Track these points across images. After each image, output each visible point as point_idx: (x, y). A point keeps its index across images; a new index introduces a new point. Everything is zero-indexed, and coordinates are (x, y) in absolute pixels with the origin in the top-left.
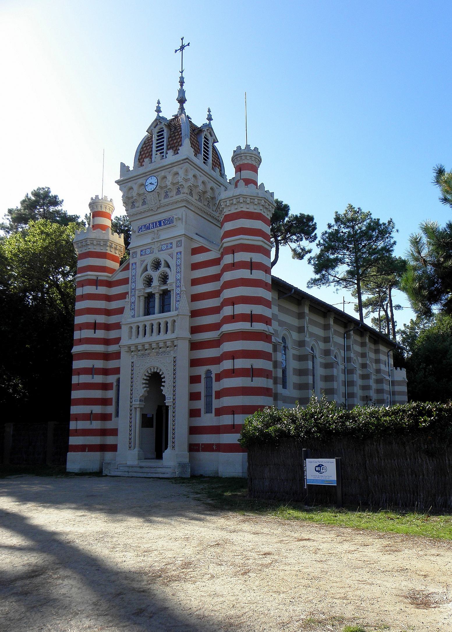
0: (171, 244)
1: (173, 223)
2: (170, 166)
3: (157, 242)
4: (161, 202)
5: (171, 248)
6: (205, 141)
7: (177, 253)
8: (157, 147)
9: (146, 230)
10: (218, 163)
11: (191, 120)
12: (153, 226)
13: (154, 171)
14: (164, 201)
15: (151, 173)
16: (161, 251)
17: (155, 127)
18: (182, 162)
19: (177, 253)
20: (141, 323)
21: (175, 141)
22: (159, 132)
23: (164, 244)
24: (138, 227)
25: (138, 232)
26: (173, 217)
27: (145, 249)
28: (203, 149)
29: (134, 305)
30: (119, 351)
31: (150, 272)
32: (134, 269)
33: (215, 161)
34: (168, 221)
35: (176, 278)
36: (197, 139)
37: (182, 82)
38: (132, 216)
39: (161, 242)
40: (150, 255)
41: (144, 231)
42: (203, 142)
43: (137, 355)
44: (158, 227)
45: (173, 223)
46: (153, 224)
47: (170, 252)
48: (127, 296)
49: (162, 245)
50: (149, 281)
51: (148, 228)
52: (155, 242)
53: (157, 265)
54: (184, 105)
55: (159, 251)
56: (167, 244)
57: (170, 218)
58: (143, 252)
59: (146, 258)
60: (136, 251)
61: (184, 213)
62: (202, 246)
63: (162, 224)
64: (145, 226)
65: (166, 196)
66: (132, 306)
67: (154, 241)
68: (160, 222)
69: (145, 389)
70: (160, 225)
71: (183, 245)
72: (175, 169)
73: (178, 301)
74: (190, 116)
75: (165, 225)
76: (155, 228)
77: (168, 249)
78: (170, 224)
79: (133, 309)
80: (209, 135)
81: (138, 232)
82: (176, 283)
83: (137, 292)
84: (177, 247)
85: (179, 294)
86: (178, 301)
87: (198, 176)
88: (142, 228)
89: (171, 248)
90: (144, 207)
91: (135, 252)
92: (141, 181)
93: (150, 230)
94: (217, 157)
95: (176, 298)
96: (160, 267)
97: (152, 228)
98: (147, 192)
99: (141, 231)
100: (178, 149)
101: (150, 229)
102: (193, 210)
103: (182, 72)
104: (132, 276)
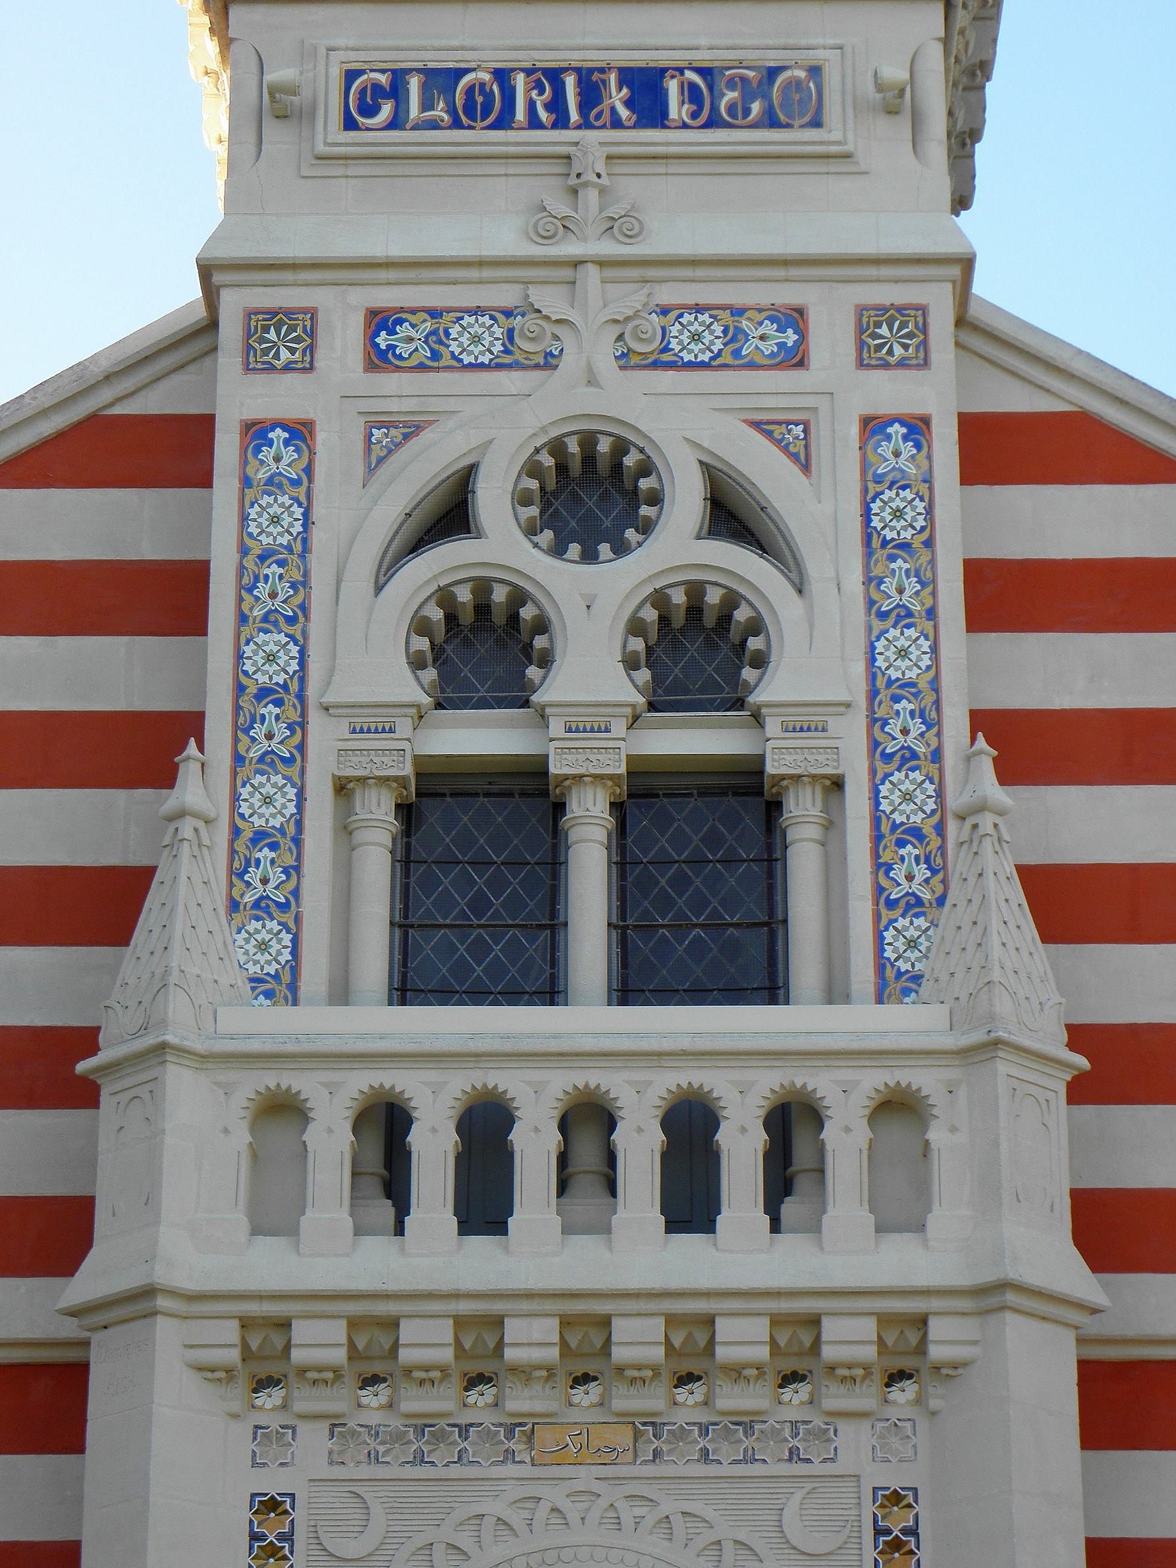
1: (816, 123)
3: (603, 263)
5: (796, 359)
9: (457, 124)
12: (557, 105)
16: (656, 365)
20: (433, 1076)
24: (351, 76)
25: (350, 124)
26: (815, 71)
27: (434, 313)
29: (294, 870)
30: (71, 1355)
32: (272, 482)
34: (749, 92)
35: (872, 678)
39: (652, 273)
41: (434, 125)
43: (335, 1425)
44: (617, 124)
47: (783, 402)
48: (192, 748)
49: (664, 311)
52: (576, 264)
55: (625, 360)
56: (737, 312)
57: (772, 73)
58: (404, 330)
59: (451, 405)
60: (313, 313)
63: (676, 108)
66: (254, 875)
67: (571, 248)
73: (914, 905)
75: (713, 122)
76: (586, 124)
77: (752, 366)
78: (771, 121)
79: (262, 907)
81: (350, 124)
82: (875, 721)
84: (861, 364)
85: (916, 833)
86: (914, 905)
88: (396, 90)
89: (796, 359)
91: (289, 313)
93: (510, 133)
95: (881, 867)
96: (646, 528)
97: (534, 123)
99: (394, 124)
101: (504, 121)
104: (244, 551)
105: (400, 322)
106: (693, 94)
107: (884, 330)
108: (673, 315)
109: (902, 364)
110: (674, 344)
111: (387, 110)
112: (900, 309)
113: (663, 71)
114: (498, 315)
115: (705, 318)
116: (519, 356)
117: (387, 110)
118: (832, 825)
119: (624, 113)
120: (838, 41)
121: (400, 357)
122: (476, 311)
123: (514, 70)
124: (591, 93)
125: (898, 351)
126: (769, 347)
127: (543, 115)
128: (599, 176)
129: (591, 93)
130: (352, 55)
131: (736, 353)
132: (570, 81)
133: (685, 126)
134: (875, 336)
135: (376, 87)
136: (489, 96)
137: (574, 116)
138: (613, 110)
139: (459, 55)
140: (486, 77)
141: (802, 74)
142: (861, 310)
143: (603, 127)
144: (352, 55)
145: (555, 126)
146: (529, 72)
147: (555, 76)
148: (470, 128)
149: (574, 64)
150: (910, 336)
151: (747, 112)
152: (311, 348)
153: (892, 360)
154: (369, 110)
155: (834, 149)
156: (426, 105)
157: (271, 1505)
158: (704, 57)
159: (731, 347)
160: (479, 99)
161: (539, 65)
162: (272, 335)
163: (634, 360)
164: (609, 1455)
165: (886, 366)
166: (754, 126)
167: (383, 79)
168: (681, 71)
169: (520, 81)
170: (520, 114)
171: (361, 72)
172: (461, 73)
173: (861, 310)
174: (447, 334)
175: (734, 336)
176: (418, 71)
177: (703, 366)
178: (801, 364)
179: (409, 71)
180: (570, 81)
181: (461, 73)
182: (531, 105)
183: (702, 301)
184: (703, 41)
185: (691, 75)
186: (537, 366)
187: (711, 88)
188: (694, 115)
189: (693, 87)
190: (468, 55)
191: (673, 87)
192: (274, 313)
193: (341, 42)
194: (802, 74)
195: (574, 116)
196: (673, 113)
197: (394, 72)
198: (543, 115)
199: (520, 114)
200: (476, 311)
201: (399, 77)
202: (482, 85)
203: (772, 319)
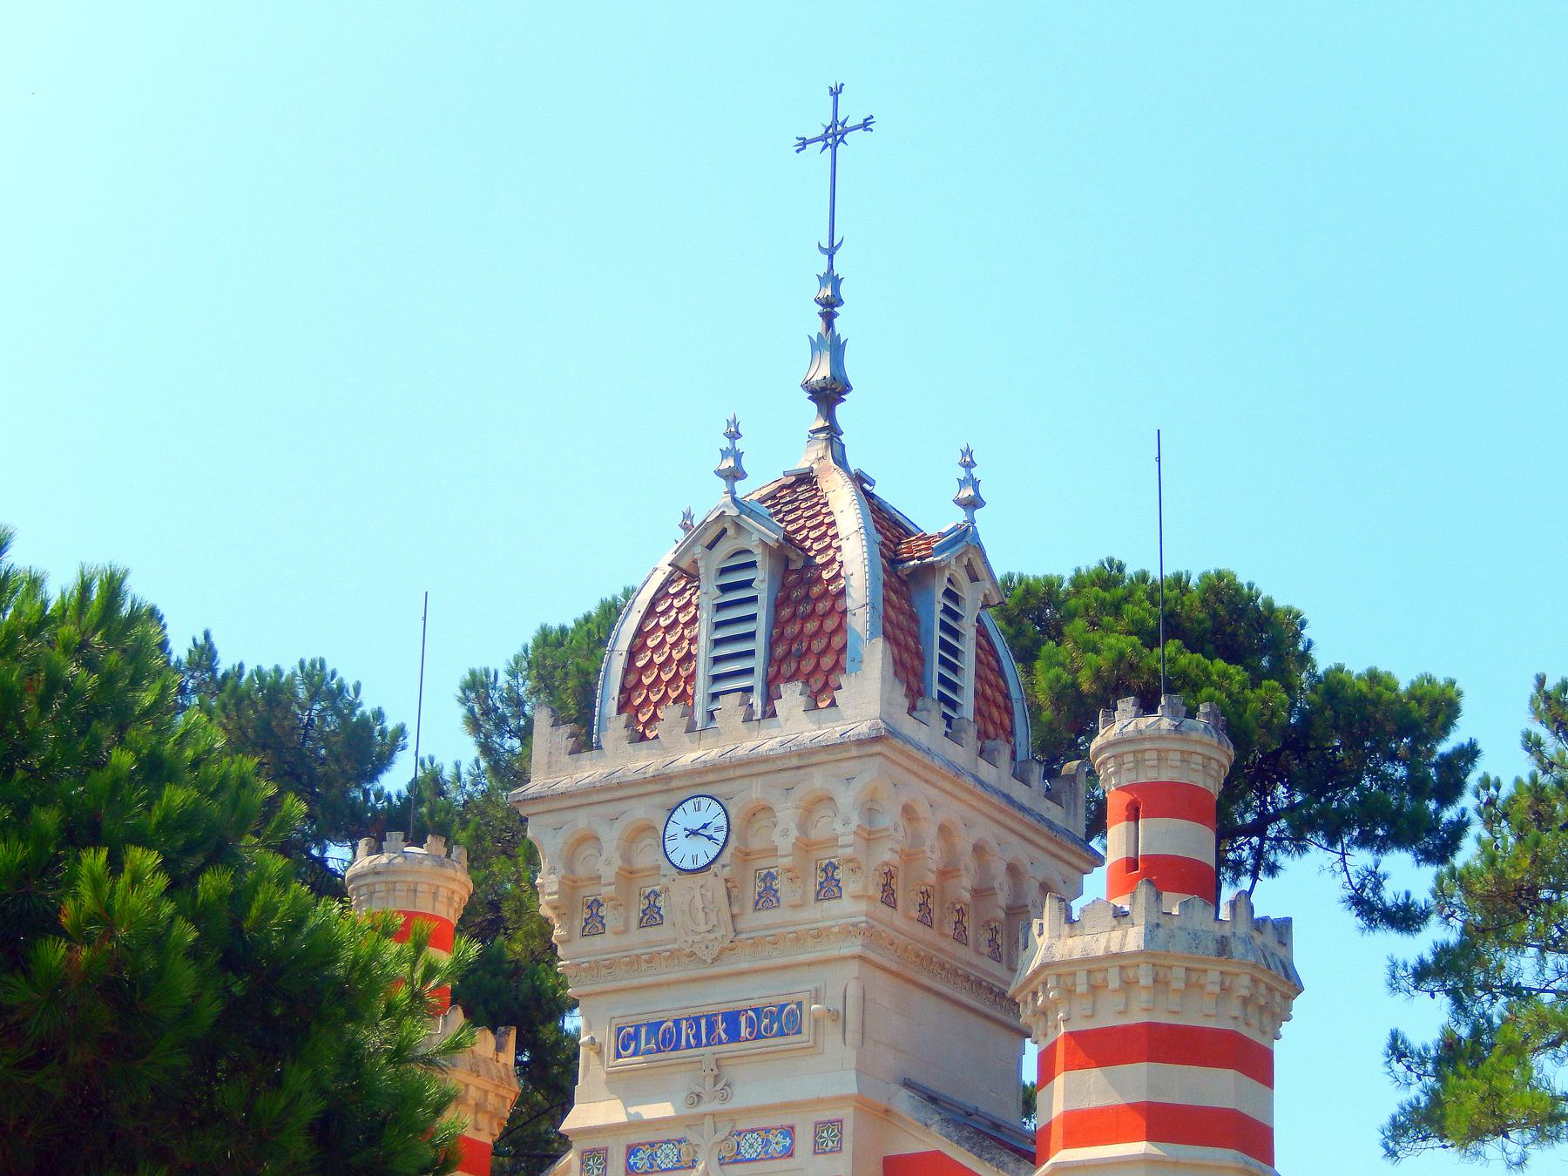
0: (790, 1131)
1: (799, 1032)
2: (795, 762)
4: (743, 924)
6: (947, 610)
8: (718, 643)
9: (659, 1051)
10: (1000, 699)
11: (876, 491)
12: (697, 1036)
13: (710, 777)
14: (754, 921)
15: (698, 780)
16: (736, 1162)
17: (711, 546)
21: (811, 626)
22: (724, 571)
23: (753, 1131)
24: (620, 1030)
25: (618, 1056)
26: (799, 1004)
27: (652, 1145)
28: (937, 651)
33: (988, 691)
34: (774, 1017)
36: (911, 606)
37: (829, 308)
38: (585, 970)
41: (650, 1052)
42: (938, 615)
44: (720, 1042)
45: (799, 1032)
46: (698, 1027)
51: (669, 1042)
54: (840, 410)
56: (767, 1130)
57: (783, 1007)
58: (640, 1154)
60: (606, 1149)
61: (853, 990)
62: (938, 1156)
63: (744, 1032)
64: (654, 1027)
65: (767, 897)
67: (703, 1108)
68: (732, 1019)
70: (734, 1035)
71: (848, 1145)
72: (818, 780)
74: (869, 471)
75: (759, 1037)
76: (708, 1044)
77: (772, 1158)
78: (781, 1033)
80: (962, 577)
84: (815, 1153)
87: (923, 810)
88: (635, 1037)
89: (789, 1153)
90: (652, 933)
92: (640, 811)
93: (679, 1052)
94: (992, 670)
97: (689, 1046)
98: (675, 871)
99: (634, 1054)
100: (832, 684)
101: (677, 1047)
102: (894, 967)
103: (831, 252)
105: (639, 1150)
106: (750, 1023)
107: (825, 1134)
108: (743, 1135)
109: (831, 1151)
110: (743, 1151)
111: (633, 1046)
112: (831, 1122)
113: (740, 1012)
114: (676, 1143)
115: (755, 1135)
116: (683, 1163)
117: (633, 1046)
119: (723, 1036)
120: (810, 988)
121: (638, 1168)
122: (668, 1142)
123: (681, 1019)
124: (711, 1027)
125: (830, 1144)
126: (779, 1148)
127: (692, 1041)
128: (712, 1070)
129: (711, 1027)
130: (620, 1020)
131: (766, 1153)
132: (703, 1022)
133: (747, 1040)
134: (821, 1137)
135: (629, 1034)
136: (671, 1034)
137: (704, 1040)
138: (719, 1035)
139: (661, 1015)
140: (671, 1024)
141: (794, 1006)
142: (816, 1124)
143: (715, 1044)
144: (620, 1020)
145: (696, 1046)
146: (687, 1019)
147: (697, 1020)
148: (664, 1051)
149: (705, 1013)
150: (835, 1136)
151: (772, 1029)
152: (605, 1167)
153: (827, 1149)
154: (625, 1048)
155: (805, 1044)
156: (648, 1042)
158: (756, 1003)
159: (764, 1150)
160: (668, 1036)
161: (692, 1016)
162: (591, 1163)
163: (727, 1160)
165: (825, 1152)
166: (774, 1036)
167: (631, 1030)
168: (746, 1011)
169: (684, 1024)
170: (683, 1042)
171: (624, 1028)
172: (661, 1023)
173: (816, 1124)
174: (656, 1155)
175: (766, 1143)
176: (645, 1024)
177: (754, 1160)
178: (791, 1155)
179: (641, 1025)
180: (703, 1022)
181: (661, 1023)
182: (688, 1035)
183: (754, 1126)
184: (755, 996)
185: (750, 1013)
186: (689, 1167)
187: (758, 1020)
188: (751, 1034)
189: (751, 1018)
190: (661, 1015)
191: (743, 1019)
192: (591, 1151)
193: (617, 1013)
194: (794, 1006)
195: (704, 1040)
196: (743, 1034)
197: (635, 1026)
198: (692, 1041)
199: (683, 1042)
200: (668, 1142)
201: (638, 1028)
202: (669, 1028)
203: (781, 1133)
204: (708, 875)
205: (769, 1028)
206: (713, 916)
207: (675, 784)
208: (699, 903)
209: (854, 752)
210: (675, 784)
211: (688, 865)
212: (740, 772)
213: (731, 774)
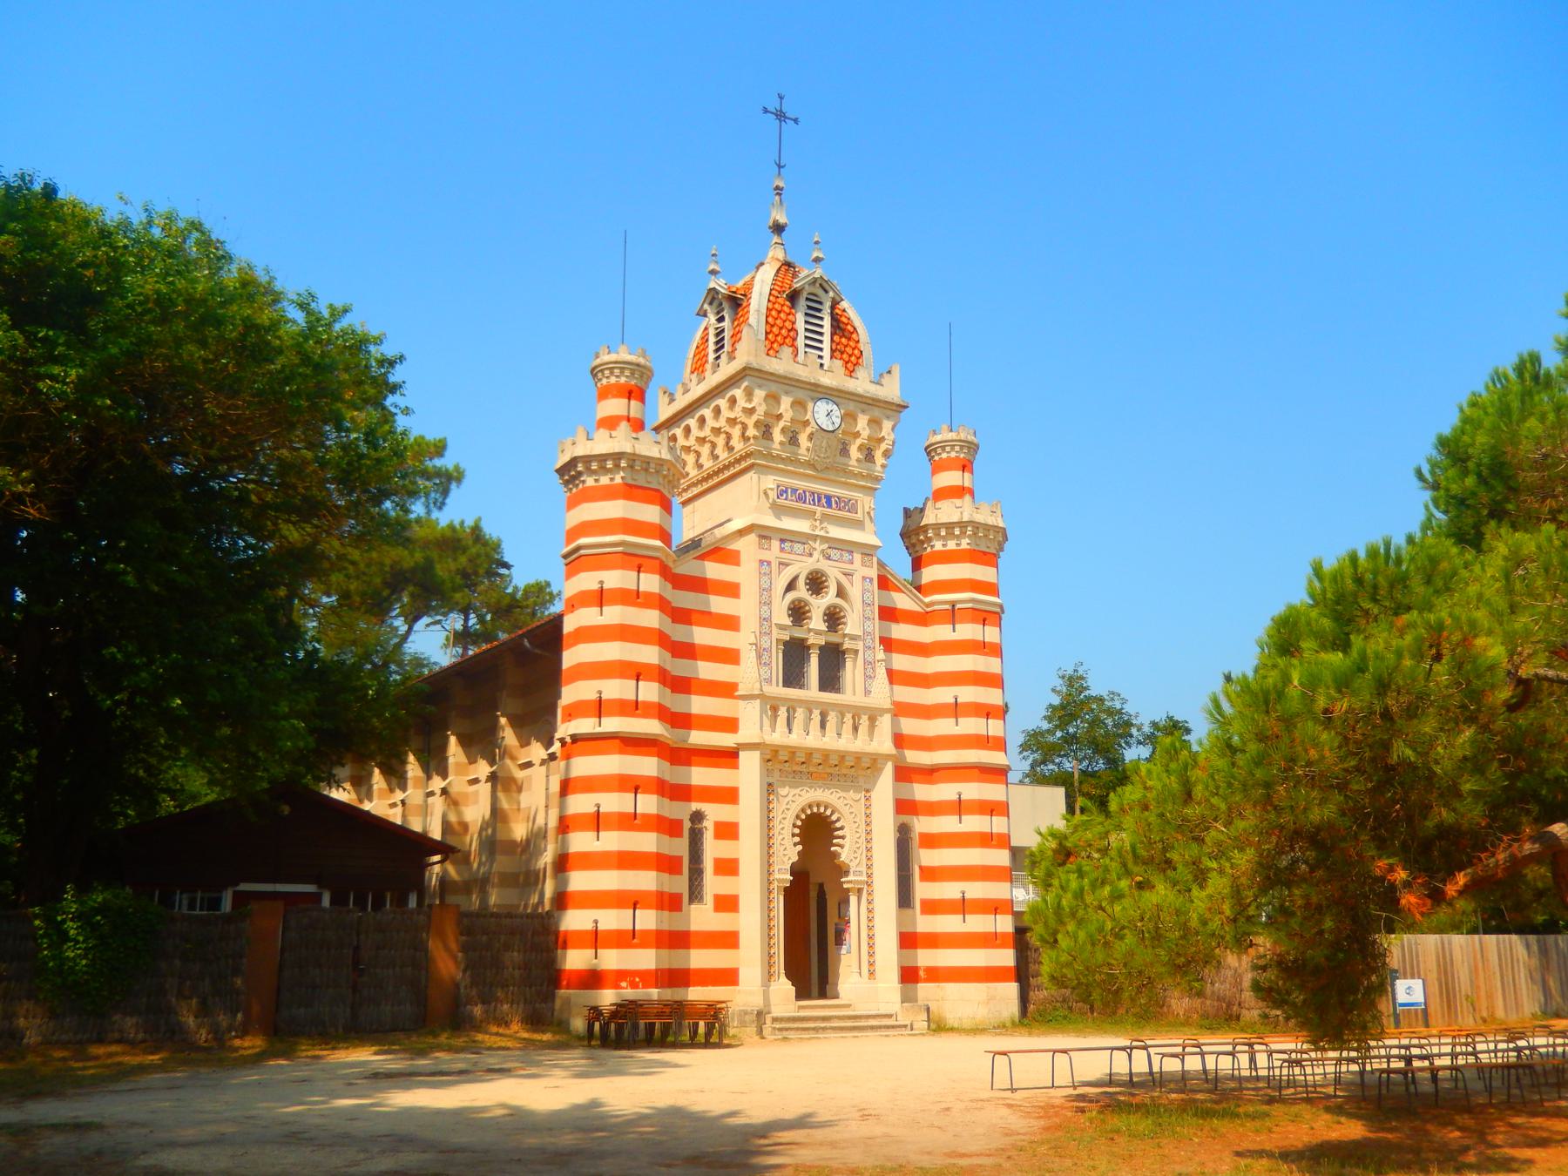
2: (871, 402)
7: (864, 578)
18: (894, 408)
19: (864, 578)
26: (856, 501)
31: (802, 592)
40: (804, 558)
50: (798, 613)
53: (816, 583)
63: (834, 505)
64: (794, 491)
67: (817, 533)
69: (800, 847)
78: (849, 511)
83: (775, 630)
88: (786, 492)
101: (804, 502)
106: (836, 503)
118: (855, 660)
124: (819, 500)
147: (813, 493)
157: (770, 785)
164: (824, 779)
204: (833, 435)
205: (844, 507)
206: (828, 454)
207: (819, 389)
208: (824, 444)
209: (894, 408)
210: (819, 389)
211: (824, 427)
212: (847, 396)
213: (843, 395)
